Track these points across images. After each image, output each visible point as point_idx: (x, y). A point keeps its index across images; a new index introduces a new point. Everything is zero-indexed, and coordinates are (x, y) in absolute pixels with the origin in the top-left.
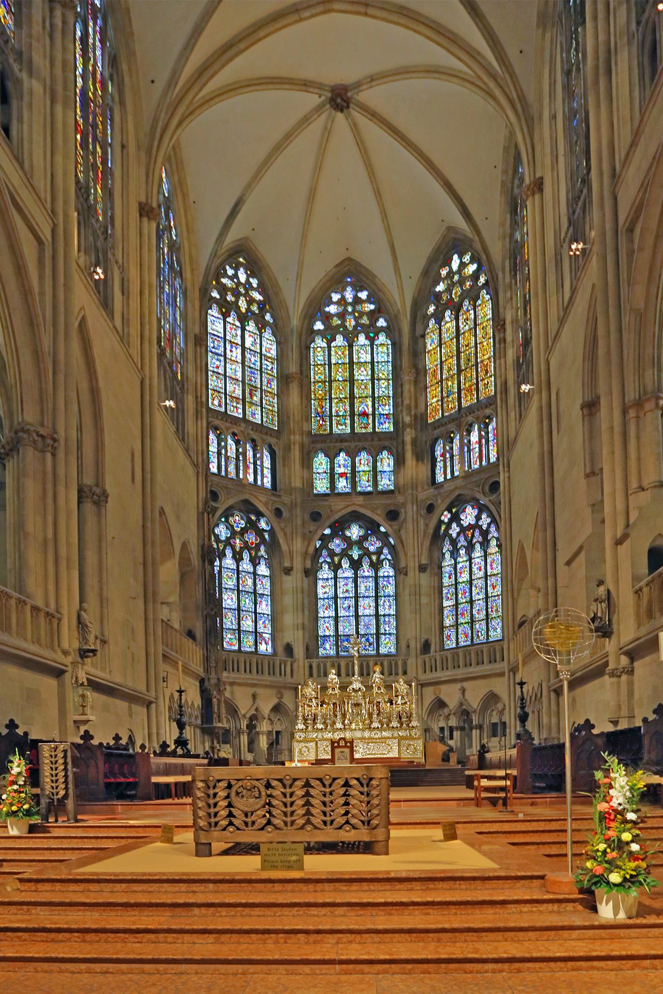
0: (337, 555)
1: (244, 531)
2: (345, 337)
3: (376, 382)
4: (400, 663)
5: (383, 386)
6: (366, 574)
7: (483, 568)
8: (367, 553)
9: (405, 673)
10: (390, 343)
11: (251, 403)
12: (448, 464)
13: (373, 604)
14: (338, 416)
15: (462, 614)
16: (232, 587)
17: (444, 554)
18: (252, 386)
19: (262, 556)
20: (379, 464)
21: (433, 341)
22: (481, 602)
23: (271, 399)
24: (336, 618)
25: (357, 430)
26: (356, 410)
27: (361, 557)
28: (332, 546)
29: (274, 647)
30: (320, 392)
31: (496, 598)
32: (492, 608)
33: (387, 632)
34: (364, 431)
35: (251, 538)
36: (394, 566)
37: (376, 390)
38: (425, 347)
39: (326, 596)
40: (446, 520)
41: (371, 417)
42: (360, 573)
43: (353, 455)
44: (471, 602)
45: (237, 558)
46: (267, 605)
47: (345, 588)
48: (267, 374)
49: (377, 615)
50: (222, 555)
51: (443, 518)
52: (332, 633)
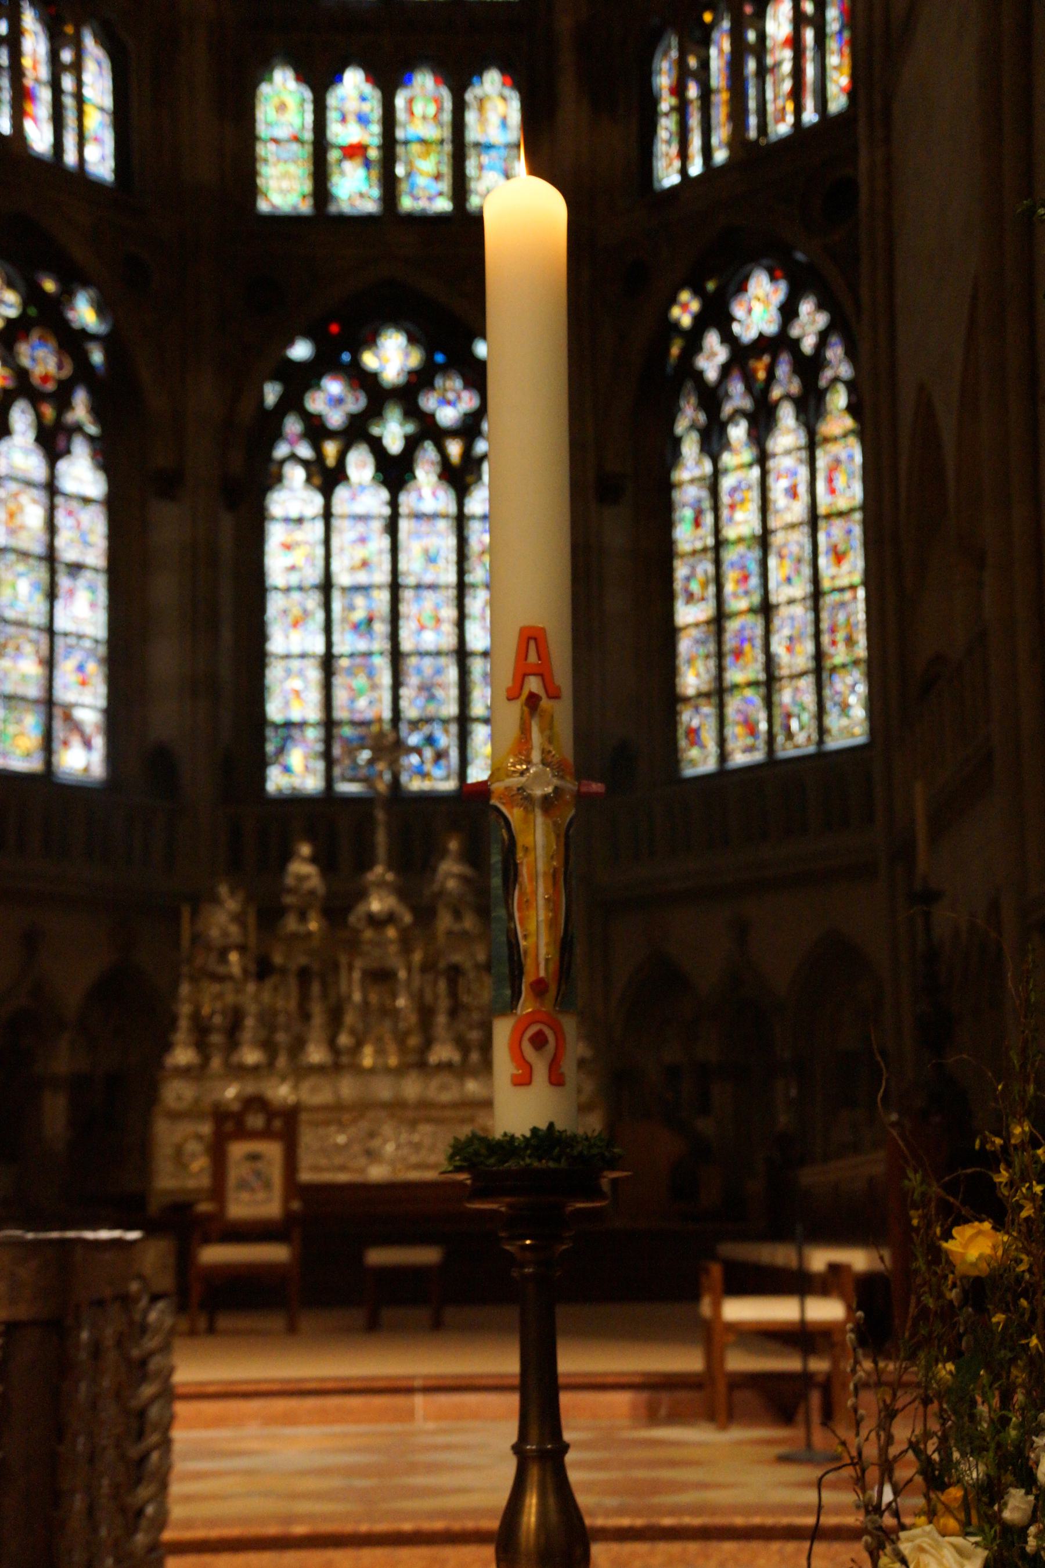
0: (331, 434)
7: (803, 490)
15: (738, 654)
17: (677, 442)
19: (78, 428)
20: (471, 117)
28: (316, 403)
29: (112, 757)
31: (848, 596)
32: (833, 630)
39: (294, 579)
40: (686, 321)
42: (407, 501)
44: (766, 609)
46: (93, 605)
51: (676, 312)
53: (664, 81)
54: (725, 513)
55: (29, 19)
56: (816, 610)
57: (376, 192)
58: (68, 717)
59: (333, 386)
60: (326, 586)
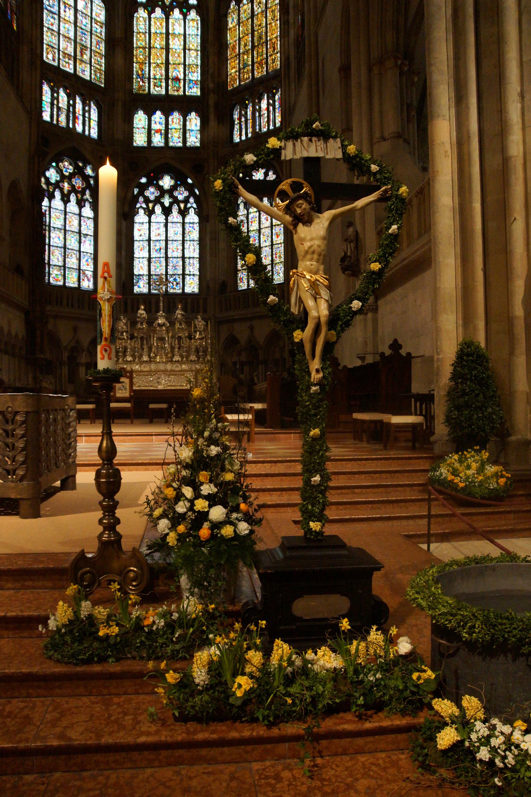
0: (151, 202)
1: (72, 176)
2: (163, 10)
3: (187, 51)
4: (201, 302)
5: (193, 56)
6: (175, 220)
8: (176, 201)
9: (205, 311)
10: (199, 18)
11: (82, 61)
12: (243, 127)
13: (180, 247)
14: (155, 79)
16: (60, 227)
17: (239, 205)
18: (82, 45)
19: (87, 200)
20: (188, 123)
21: (233, 20)
22: (267, 249)
23: (99, 59)
24: (149, 260)
25: (171, 92)
26: (170, 74)
27: (171, 204)
28: (147, 193)
30: (141, 57)
33: (192, 273)
34: (176, 93)
35: (78, 183)
36: (198, 213)
37: (187, 58)
38: (227, 25)
39: (141, 238)
41: (182, 82)
42: (170, 219)
43: (167, 114)
45: (66, 200)
46: (90, 245)
47: (158, 232)
48: (97, 36)
49: (183, 258)
50: (51, 197)
52: (146, 272)
53: (236, 116)
54: (250, 223)
55: (78, 100)
56: (272, 249)
57: (163, 141)
58: (84, 273)
59: (152, 189)
60: (149, 240)
